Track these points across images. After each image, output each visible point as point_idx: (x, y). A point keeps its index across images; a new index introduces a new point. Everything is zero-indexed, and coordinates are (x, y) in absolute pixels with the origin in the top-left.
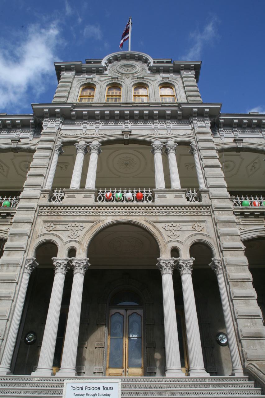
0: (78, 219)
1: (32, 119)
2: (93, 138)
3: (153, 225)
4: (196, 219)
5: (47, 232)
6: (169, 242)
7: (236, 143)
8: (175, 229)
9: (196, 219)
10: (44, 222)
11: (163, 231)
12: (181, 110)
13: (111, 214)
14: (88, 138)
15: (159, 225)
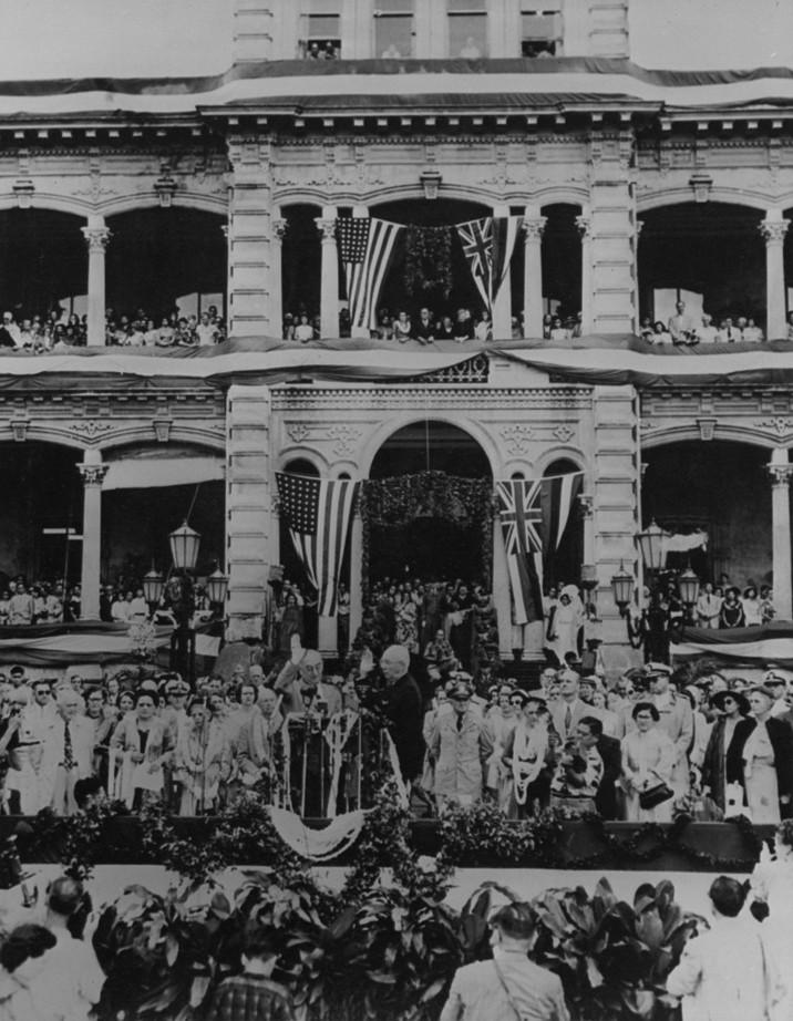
0: (345, 416)
1: (197, 128)
2: (352, 196)
3: (483, 429)
4: (562, 416)
5: (295, 445)
6: (508, 463)
7: (694, 188)
8: (521, 436)
9: (562, 416)
10: (287, 422)
11: (498, 439)
12: (563, 115)
13: (407, 405)
14: (340, 196)
15: (494, 430)
